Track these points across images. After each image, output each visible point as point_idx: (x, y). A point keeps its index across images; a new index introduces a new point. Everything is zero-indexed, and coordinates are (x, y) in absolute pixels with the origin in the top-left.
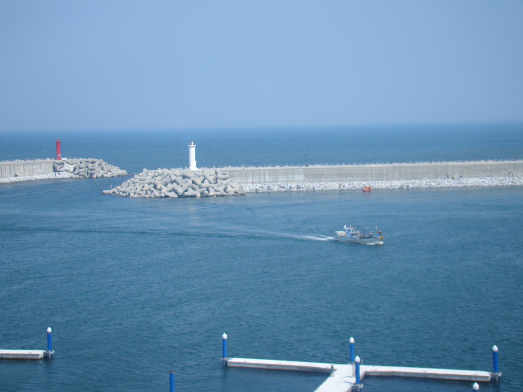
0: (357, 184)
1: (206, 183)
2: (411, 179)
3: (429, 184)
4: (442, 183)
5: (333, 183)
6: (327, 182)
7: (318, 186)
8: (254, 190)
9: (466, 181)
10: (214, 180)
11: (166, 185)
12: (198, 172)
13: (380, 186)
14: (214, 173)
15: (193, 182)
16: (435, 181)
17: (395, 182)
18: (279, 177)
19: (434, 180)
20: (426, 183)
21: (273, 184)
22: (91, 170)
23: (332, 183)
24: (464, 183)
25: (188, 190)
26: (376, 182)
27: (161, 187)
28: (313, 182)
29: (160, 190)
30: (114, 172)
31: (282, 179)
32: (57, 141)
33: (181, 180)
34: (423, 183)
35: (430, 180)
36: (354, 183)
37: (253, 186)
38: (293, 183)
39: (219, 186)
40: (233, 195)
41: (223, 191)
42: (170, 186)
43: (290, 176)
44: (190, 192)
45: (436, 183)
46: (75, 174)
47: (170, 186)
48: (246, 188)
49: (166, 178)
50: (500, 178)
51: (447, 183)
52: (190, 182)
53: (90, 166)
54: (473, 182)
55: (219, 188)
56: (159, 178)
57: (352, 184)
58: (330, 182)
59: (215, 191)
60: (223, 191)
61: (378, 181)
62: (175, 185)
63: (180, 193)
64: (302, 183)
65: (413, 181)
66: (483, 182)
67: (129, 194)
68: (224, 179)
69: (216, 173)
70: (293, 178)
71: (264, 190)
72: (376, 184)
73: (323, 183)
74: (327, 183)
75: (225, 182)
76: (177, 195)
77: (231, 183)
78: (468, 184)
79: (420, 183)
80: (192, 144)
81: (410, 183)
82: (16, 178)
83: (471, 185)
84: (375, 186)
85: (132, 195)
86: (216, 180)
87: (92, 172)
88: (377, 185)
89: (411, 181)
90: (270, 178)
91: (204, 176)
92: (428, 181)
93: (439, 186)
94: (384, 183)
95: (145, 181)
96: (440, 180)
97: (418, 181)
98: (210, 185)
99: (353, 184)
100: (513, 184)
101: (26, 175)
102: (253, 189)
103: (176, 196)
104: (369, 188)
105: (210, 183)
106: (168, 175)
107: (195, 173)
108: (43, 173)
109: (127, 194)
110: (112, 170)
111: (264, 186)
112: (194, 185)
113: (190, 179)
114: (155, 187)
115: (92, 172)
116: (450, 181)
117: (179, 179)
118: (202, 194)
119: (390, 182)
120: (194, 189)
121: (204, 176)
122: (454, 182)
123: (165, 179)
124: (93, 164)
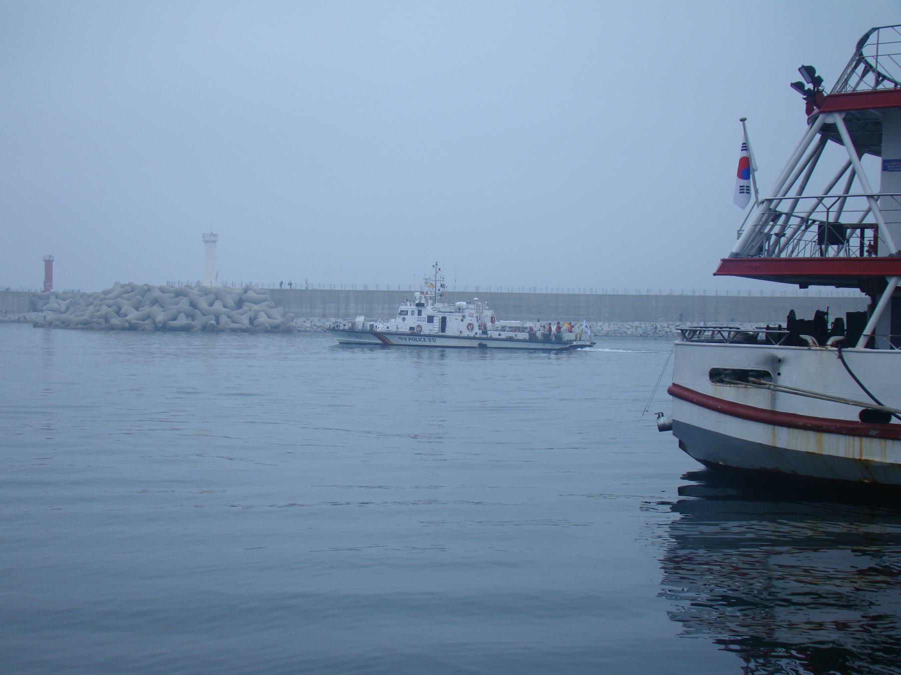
1: (218, 306)
2: (633, 321)
3: (668, 330)
8: (319, 327)
17: (600, 324)
35: (671, 323)
39: (242, 315)
44: (182, 321)
47: (146, 309)
52: (184, 303)
59: (232, 322)
65: (637, 323)
68: (256, 302)
75: (256, 307)
76: (154, 326)
86: (240, 303)
89: (630, 323)
97: (645, 324)
102: (317, 325)
113: (185, 298)
120: (192, 317)
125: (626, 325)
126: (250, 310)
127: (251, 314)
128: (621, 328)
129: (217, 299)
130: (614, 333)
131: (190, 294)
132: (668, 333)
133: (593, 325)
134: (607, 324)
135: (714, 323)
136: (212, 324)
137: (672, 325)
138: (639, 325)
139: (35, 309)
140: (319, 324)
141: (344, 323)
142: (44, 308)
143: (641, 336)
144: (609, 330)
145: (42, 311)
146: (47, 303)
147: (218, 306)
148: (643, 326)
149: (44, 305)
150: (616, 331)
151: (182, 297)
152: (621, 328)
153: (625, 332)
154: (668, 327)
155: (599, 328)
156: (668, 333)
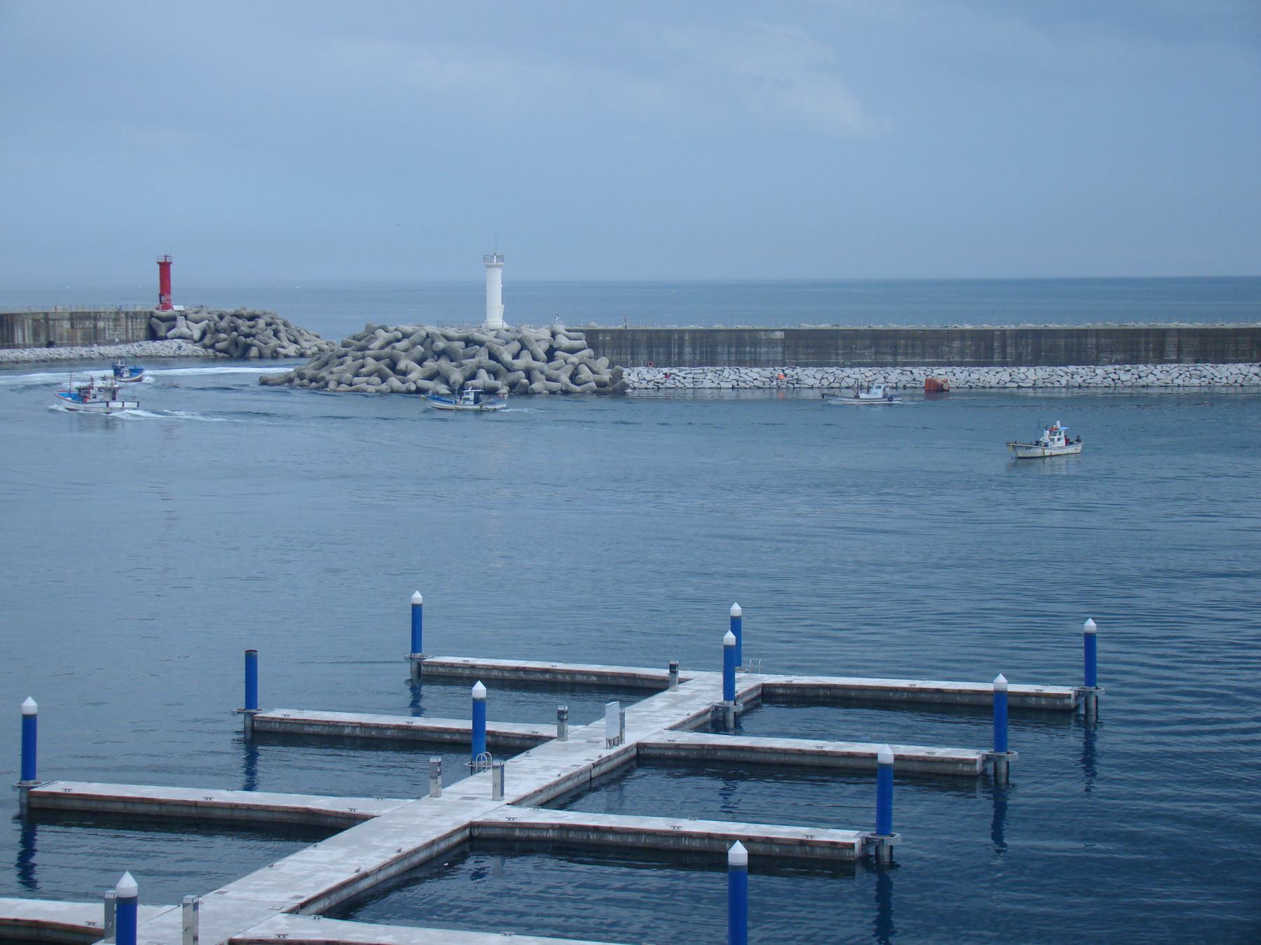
0: (922, 372)
1: (525, 360)
2: (1066, 365)
3: (1115, 377)
4: (1147, 376)
5: (860, 371)
6: (844, 366)
7: (819, 376)
8: (650, 381)
9: (1212, 370)
10: (546, 353)
11: (420, 362)
12: (508, 331)
13: (981, 379)
14: (545, 334)
15: (492, 356)
16: (1129, 371)
17: (1023, 369)
18: (719, 350)
19: (1126, 369)
20: (1106, 376)
21: (703, 370)
22: (247, 336)
23: (856, 369)
24: (1205, 377)
25: (477, 376)
27: (406, 366)
28: (807, 365)
29: (405, 373)
30: (305, 344)
31: (725, 357)
32: (162, 260)
33: (462, 351)
34: (1097, 375)
35: (1117, 367)
36: (914, 371)
37: (650, 371)
38: (755, 367)
40: (595, 392)
41: (567, 381)
42: (430, 364)
43: (748, 349)
44: (484, 379)
45: (1133, 374)
46: (205, 347)
47: (430, 364)
48: (631, 377)
49: (422, 345)
51: (1160, 376)
52: (483, 357)
53: (244, 326)
54: (1231, 374)
55: (558, 372)
56: (404, 344)
57: (909, 373)
58: (852, 366)
59: (549, 379)
60: (569, 381)
61: (976, 368)
62: (444, 364)
63: (454, 383)
64: (776, 368)
65: (1072, 368)
66: (1256, 375)
67: (327, 384)
68: (572, 351)
69: (554, 335)
70: (755, 352)
71: (678, 384)
72: (972, 374)
73: (830, 370)
74: (844, 369)
75: (574, 359)
76: (446, 387)
77: (592, 362)
78: (1216, 380)
79: (1089, 373)
80: (495, 261)
81: (1063, 374)
82: (52, 350)
83: (1224, 381)
84: (968, 378)
85: (332, 385)
86: (551, 354)
87: (249, 340)
88: (974, 376)
89: (1062, 368)
90: (695, 353)
91: (520, 341)
92: (1110, 368)
93: (1141, 382)
94: (992, 373)
95: (368, 352)
96: (1142, 367)
97: (1083, 369)
98: (535, 364)
99: (911, 372)
101: (77, 345)
102: (648, 379)
103: (443, 389)
104: (946, 381)
105: (535, 359)
106: (428, 336)
107: (498, 334)
108: (121, 342)
109: (322, 383)
110: (300, 340)
111: (679, 374)
112: (493, 362)
114: (393, 366)
115: (249, 340)
116: (1168, 372)
117: (459, 345)
118: (512, 386)
119: (1009, 370)
120: (495, 374)
121: (520, 341)
122: (1181, 374)
123: (419, 347)
124: (251, 323)
125: (1059, 370)
126: (565, 361)
127: (570, 368)
128: (1052, 375)
129: (522, 349)
130: (1044, 382)
131: (487, 343)
132: (1116, 381)
133: (1013, 372)
134: (1032, 370)
135: (1177, 365)
136: (523, 385)
137: (1120, 370)
138: (1075, 370)
139: (153, 335)
140: (648, 377)
141: (682, 374)
142: (170, 334)
143: (1080, 385)
144: (1035, 378)
145: (166, 338)
146: (173, 327)
147: (525, 360)
148: (1081, 371)
149: (169, 330)
150: (1045, 380)
151: (477, 347)
152: (1052, 375)
153: (1058, 381)
154: (1115, 373)
155: (1023, 376)
156: (1116, 381)
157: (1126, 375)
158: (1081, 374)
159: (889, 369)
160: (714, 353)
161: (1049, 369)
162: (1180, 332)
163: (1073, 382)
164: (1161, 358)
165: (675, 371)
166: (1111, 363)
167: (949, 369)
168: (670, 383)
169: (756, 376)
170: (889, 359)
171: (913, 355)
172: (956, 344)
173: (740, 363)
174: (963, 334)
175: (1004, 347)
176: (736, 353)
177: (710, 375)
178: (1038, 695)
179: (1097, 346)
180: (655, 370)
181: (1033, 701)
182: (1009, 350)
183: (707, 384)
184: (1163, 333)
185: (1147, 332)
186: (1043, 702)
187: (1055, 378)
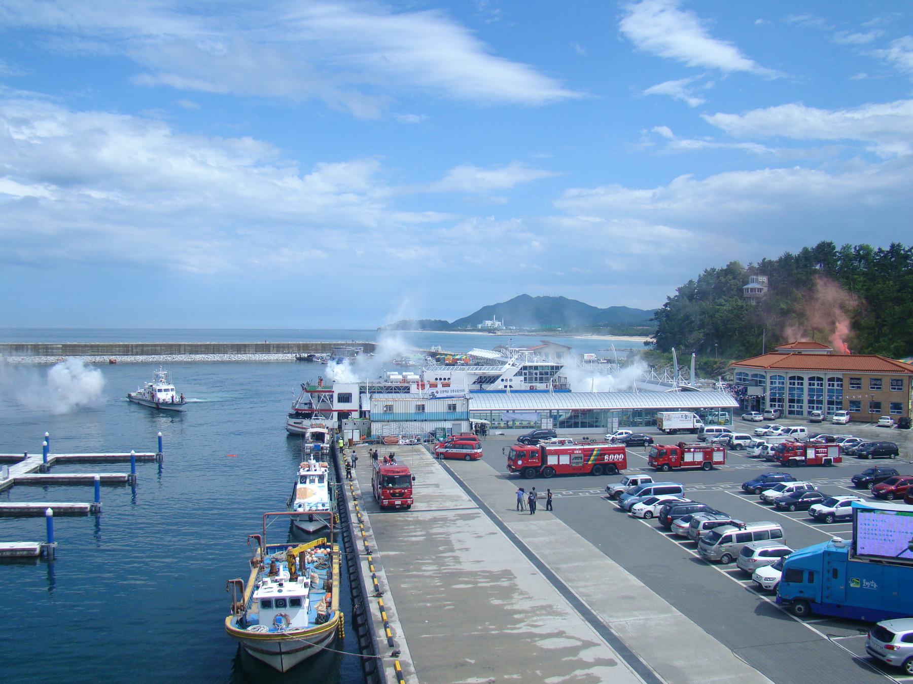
2: (151, 355)
17: (138, 356)
26: (123, 356)
43: (50, 351)
50: (220, 355)
58: (84, 356)
65: (153, 356)
92: (165, 356)
96: (174, 356)
100: (230, 359)
119: (134, 356)
140: (16, 360)
157: (169, 358)
158: (156, 358)
159: (96, 357)
160: (39, 352)
161: (147, 356)
162: (185, 345)
163: (153, 360)
164: (180, 353)
165: (25, 358)
166: (165, 354)
167: (115, 356)
168: (23, 362)
169: (52, 359)
170: (96, 353)
171: (104, 352)
172: (117, 349)
173: (47, 355)
174: (119, 346)
175: (132, 350)
176: (46, 352)
177: (37, 359)
178: (144, 456)
179: (161, 349)
180: (18, 358)
181: (143, 458)
182: (134, 351)
183: (36, 361)
184: (180, 345)
185: (175, 345)
186: (146, 458)
187: (148, 359)
